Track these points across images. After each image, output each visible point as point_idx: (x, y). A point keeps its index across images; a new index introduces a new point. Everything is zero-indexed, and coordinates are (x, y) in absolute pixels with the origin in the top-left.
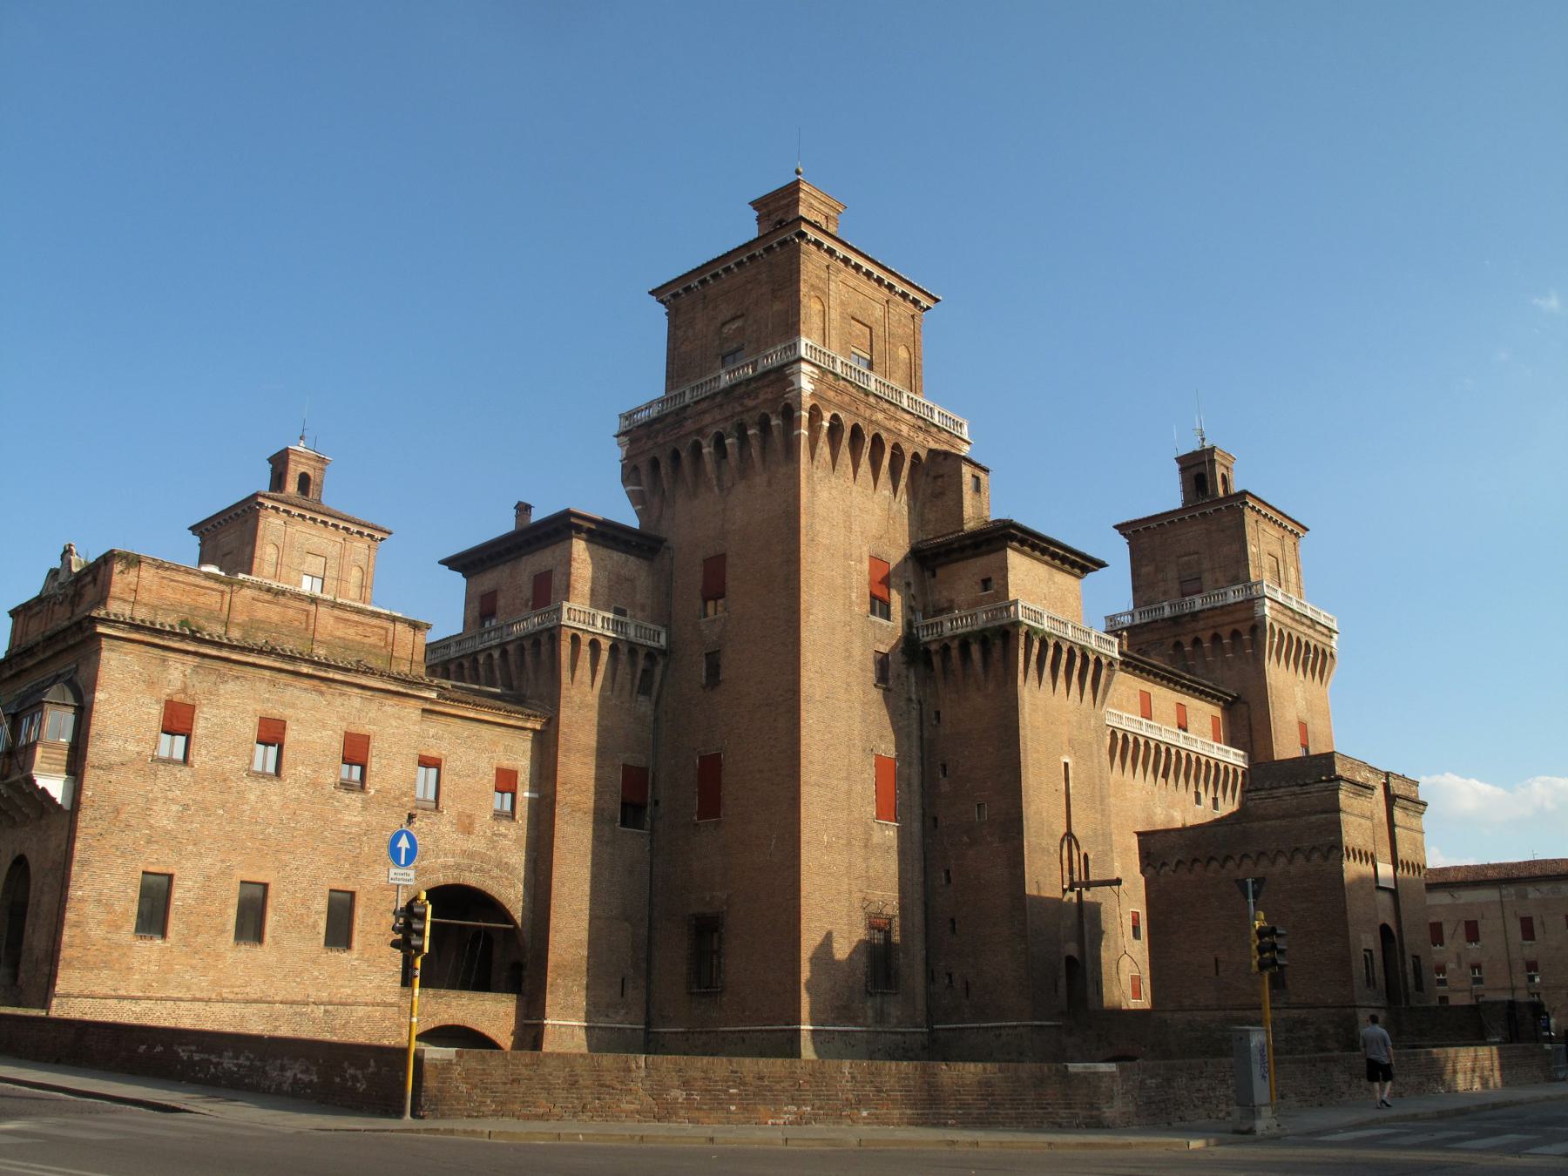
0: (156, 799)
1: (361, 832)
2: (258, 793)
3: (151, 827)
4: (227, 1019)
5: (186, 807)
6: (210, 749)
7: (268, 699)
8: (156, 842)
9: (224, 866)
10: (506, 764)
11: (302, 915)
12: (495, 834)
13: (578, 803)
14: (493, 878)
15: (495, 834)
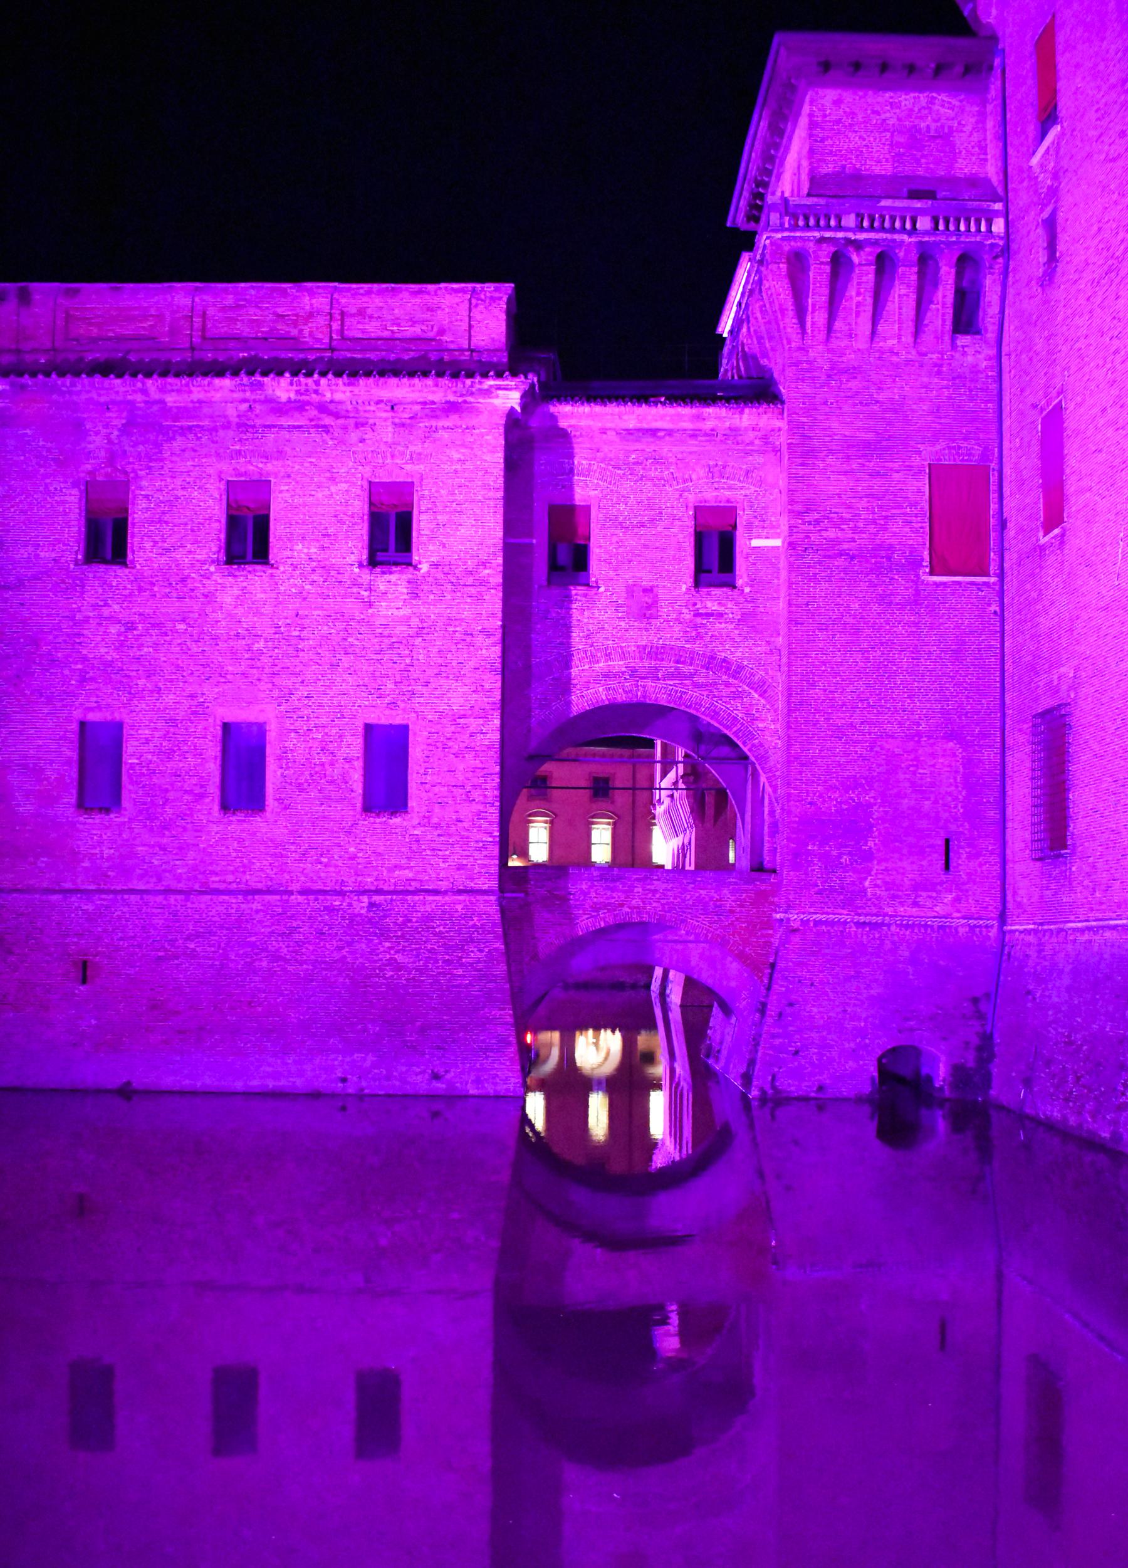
0: (86, 620)
1: (411, 632)
2: (236, 592)
3: (85, 659)
4: (217, 919)
5: (131, 626)
6: (157, 539)
7: (239, 452)
8: (93, 679)
9: (194, 703)
10: (711, 496)
11: (322, 764)
12: (700, 615)
13: (836, 542)
14: (696, 685)
15: (700, 615)
